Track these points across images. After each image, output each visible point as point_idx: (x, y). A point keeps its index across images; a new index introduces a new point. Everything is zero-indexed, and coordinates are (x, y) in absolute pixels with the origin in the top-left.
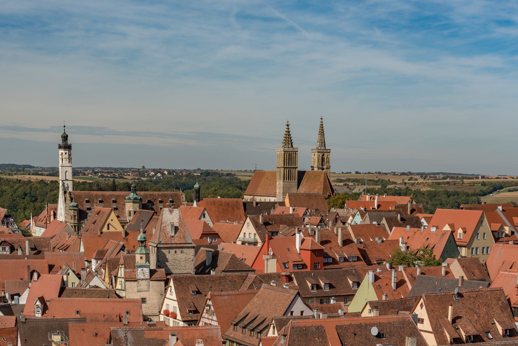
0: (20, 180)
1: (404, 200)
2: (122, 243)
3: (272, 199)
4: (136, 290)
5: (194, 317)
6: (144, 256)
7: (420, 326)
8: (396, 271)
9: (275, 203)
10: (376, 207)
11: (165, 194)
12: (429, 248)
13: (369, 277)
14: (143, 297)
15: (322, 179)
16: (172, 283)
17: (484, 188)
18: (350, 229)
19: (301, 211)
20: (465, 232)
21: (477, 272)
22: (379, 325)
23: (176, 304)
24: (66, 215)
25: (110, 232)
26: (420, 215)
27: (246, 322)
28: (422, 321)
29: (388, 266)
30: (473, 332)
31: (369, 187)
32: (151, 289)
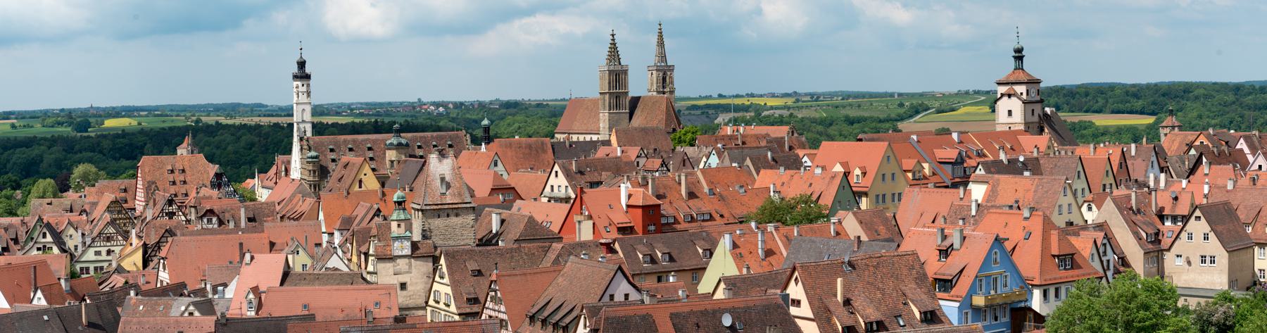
1: (781, 131)
2: (376, 207)
3: (595, 138)
4: (391, 271)
5: (476, 309)
6: (403, 225)
7: (793, 311)
8: (763, 233)
9: (598, 141)
10: (739, 142)
12: (814, 198)
13: (725, 242)
14: (403, 281)
15: (664, 107)
16: (442, 261)
17: (901, 111)
18: (699, 174)
19: (633, 152)
20: (864, 174)
21: (882, 229)
22: (732, 311)
23: (448, 290)
26: (801, 152)
27: (546, 313)
28: (797, 303)
29: (753, 224)
30: (874, 315)
31: (736, 115)
32: (414, 270)
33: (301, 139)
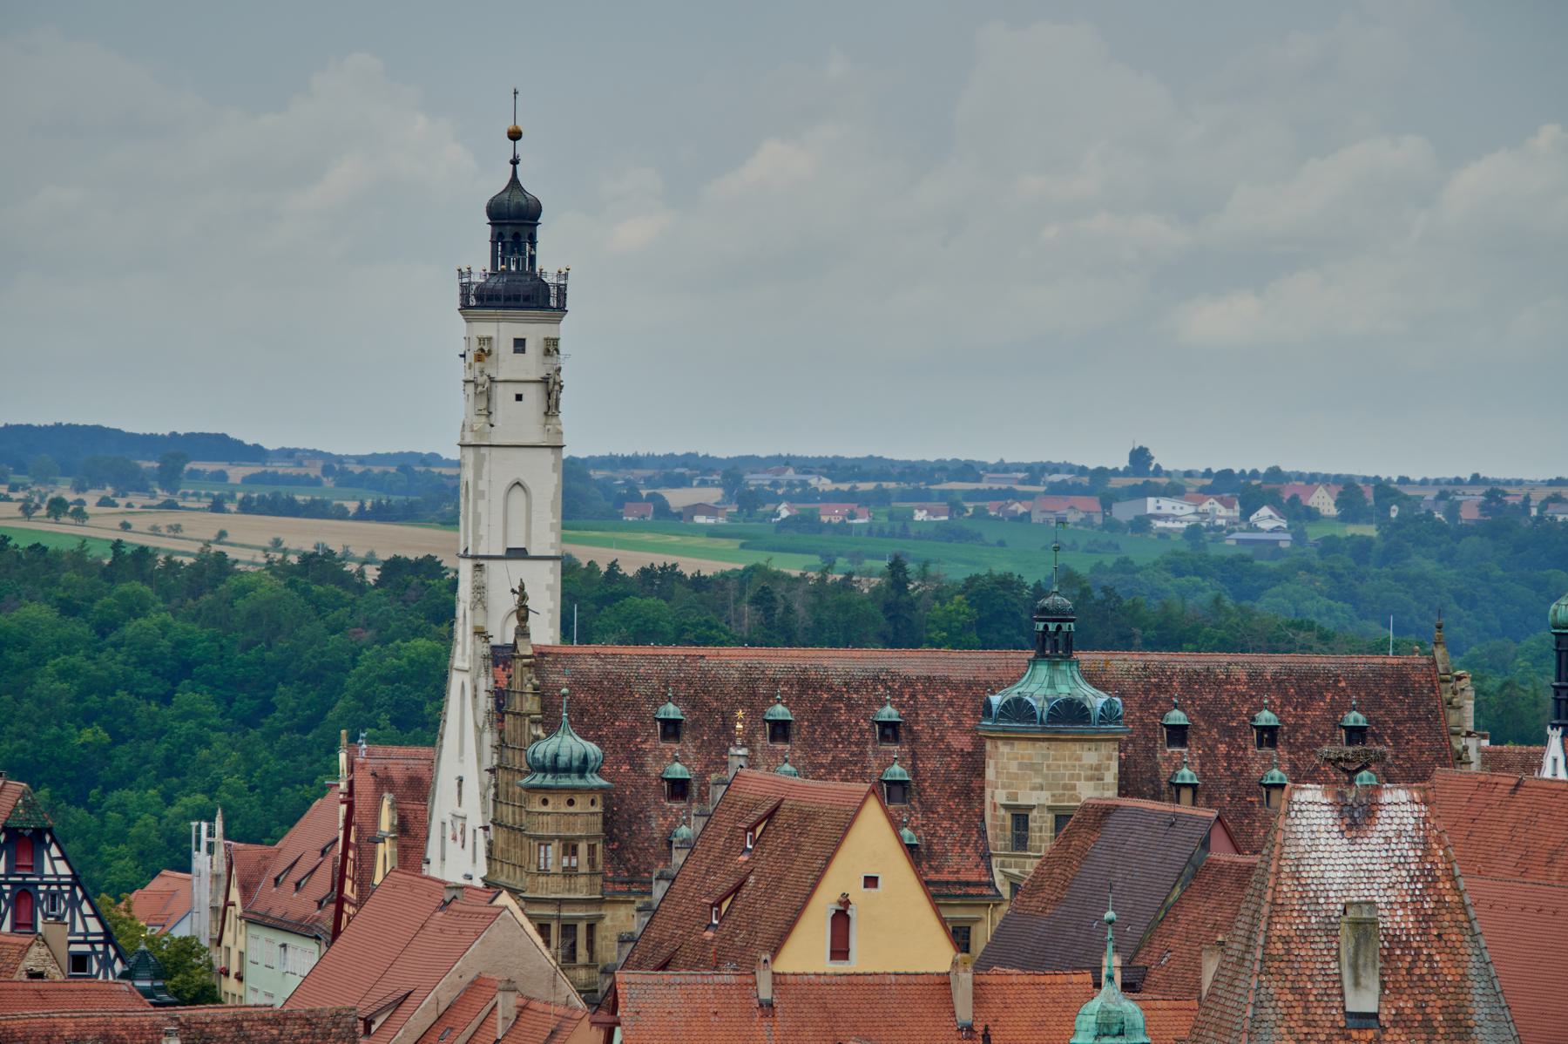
0: (143, 553)
11: (1311, 675)
24: (500, 838)
25: (854, 980)
33: (501, 657)
